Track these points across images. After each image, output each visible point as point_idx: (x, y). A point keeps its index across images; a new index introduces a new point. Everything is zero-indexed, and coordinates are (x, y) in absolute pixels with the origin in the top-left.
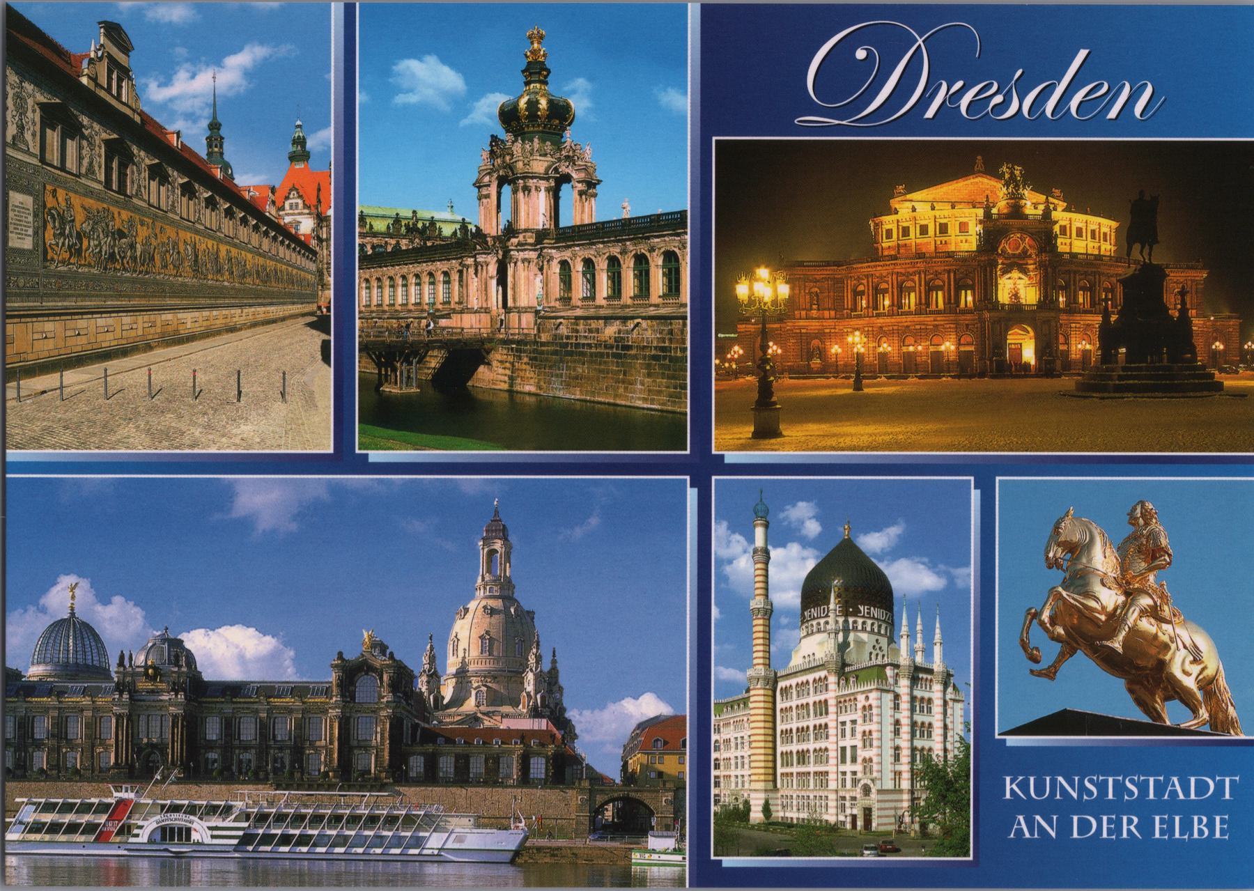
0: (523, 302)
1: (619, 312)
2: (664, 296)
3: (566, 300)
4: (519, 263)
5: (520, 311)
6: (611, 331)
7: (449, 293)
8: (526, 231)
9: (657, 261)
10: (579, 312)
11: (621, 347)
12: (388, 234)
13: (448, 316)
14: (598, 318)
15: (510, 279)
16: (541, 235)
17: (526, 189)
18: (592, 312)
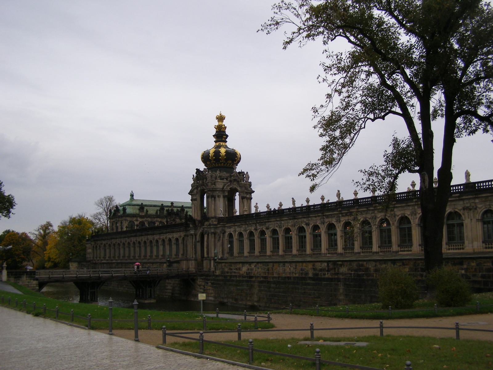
4: (210, 235)
8: (212, 218)
15: (205, 243)
16: (220, 220)
17: (213, 197)
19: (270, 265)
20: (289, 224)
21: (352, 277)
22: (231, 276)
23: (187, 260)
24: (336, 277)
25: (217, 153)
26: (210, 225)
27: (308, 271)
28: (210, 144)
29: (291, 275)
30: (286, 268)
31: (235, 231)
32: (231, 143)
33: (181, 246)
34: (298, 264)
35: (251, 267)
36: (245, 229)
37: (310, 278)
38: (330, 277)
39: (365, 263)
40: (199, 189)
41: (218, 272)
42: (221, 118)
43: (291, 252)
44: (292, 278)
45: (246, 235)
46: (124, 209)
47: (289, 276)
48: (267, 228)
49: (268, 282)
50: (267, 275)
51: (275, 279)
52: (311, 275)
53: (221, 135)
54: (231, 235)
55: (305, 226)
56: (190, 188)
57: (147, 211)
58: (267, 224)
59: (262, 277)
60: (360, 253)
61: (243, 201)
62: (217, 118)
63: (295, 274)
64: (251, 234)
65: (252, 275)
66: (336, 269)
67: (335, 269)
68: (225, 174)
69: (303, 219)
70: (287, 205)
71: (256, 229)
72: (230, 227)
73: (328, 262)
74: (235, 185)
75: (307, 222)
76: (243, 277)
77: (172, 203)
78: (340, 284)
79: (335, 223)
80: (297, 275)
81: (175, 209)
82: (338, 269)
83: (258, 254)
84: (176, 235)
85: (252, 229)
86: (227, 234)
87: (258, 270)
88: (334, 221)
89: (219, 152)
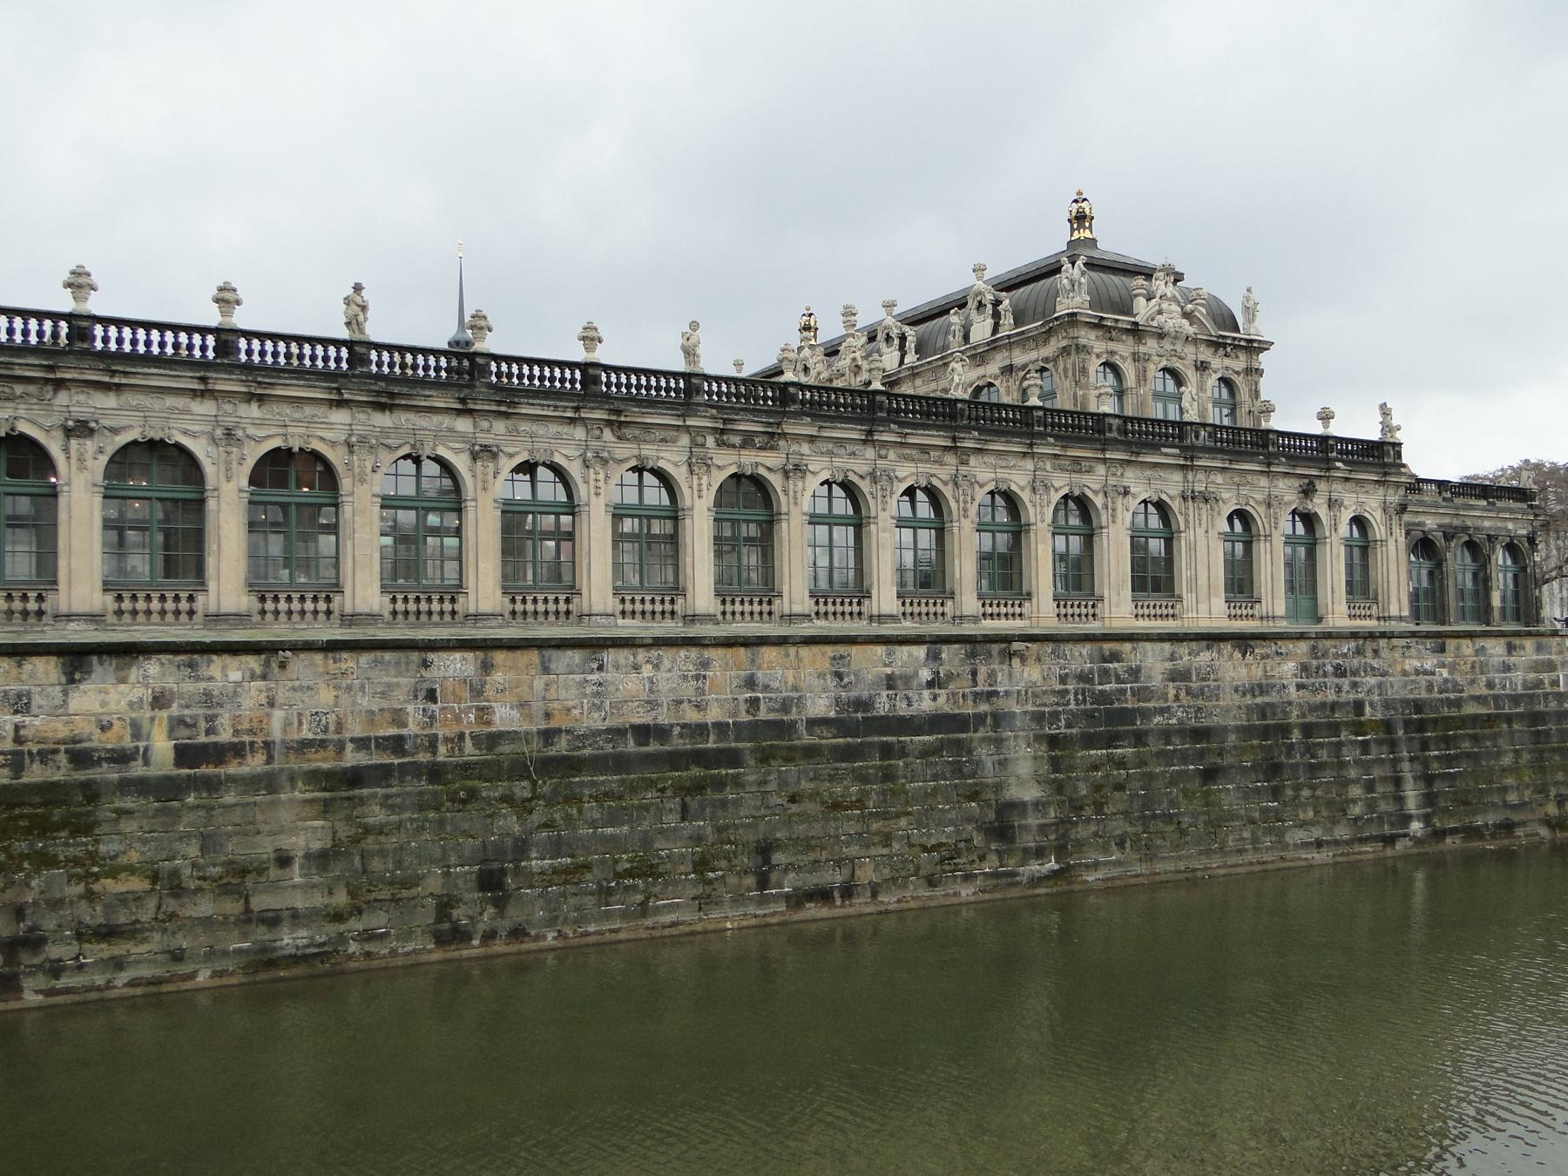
21: (1068, 703)
24: (984, 707)
27: (795, 689)
30: (608, 676)
35: (198, 679)
37: (813, 723)
38: (947, 709)
39: (1127, 646)
44: (677, 730)
52: (820, 705)
59: (362, 743)
65: (225, 736)
66: (981, 677)
67: (974, 673)
69: (446, 421)
75: (484, 439)
78: (1016, 737)
80: (714, 715)
82: (992, 675)
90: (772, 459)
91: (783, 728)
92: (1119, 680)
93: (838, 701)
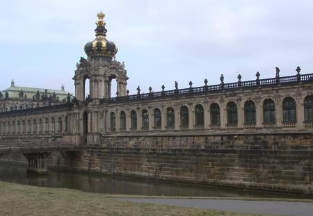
0: (95, 130)
1: (136, 134)
2: (131, 129)
3: (113, 129)
5: (93, 134)
6: (132, 143)
7: (61, 127)
8: (95, 99)
9: (150, 113)
10: (119, 135)
11: (137, 151)
12: (34, 100)
13: (61, 137)
14: (127, 137)
15: (89, 121)
16: (102, 101)
17: (96, 81)
18: (124, 134)
19: (160, 139)
20: (172, 103)
22: (118, 149)
23: (70, 134)
25: (99, 45)
26: (93, 105)
28: (92, 37)
29: (182, 148)
31: (117, 110)
32: (110, 37)
33: (64, 124)
34: (189, 138)
36: (128, 110)
37: (202, 150)
39: (262, 137)
40: (83, 75)
41: (104, 145)
42: (101, 16)
43: (188, 127)
45: (128, 114)
46: (7, 94)
47: (179, 148)
48: (150, 108)
49: (158, 154)
50: (156, 148)
51: (164, 152)
52: (203, 147)
53: (101, 30)
54: (112, 113)
55: (187, 106)
56: (74, 74)
57: (26, 96)
58: (149, 105)
60: (243, 129)
61: (120, 87)
62: (98, 16)
63: (186, 146)
64: (133, 113)
67: (229, 142)
68: (106, 63)
70: (170, 87)
71: (138, 109)
72: (111, 107)
73: (222, 136)
74: (114, 72)
76: (131, 149)
77: (46, 90)
79: (219, 103)
80: (188, 148)
81: (49, 96)
83: (140, 130)
84: (59, 114)
85: (135, 108)
86: (109, 113)
87: (148, 144)
88: (217, 101)
89: (101, 44)
90: (235, 98)
91: (197, 151)
92: (261, 144)
93: (206, 146)
